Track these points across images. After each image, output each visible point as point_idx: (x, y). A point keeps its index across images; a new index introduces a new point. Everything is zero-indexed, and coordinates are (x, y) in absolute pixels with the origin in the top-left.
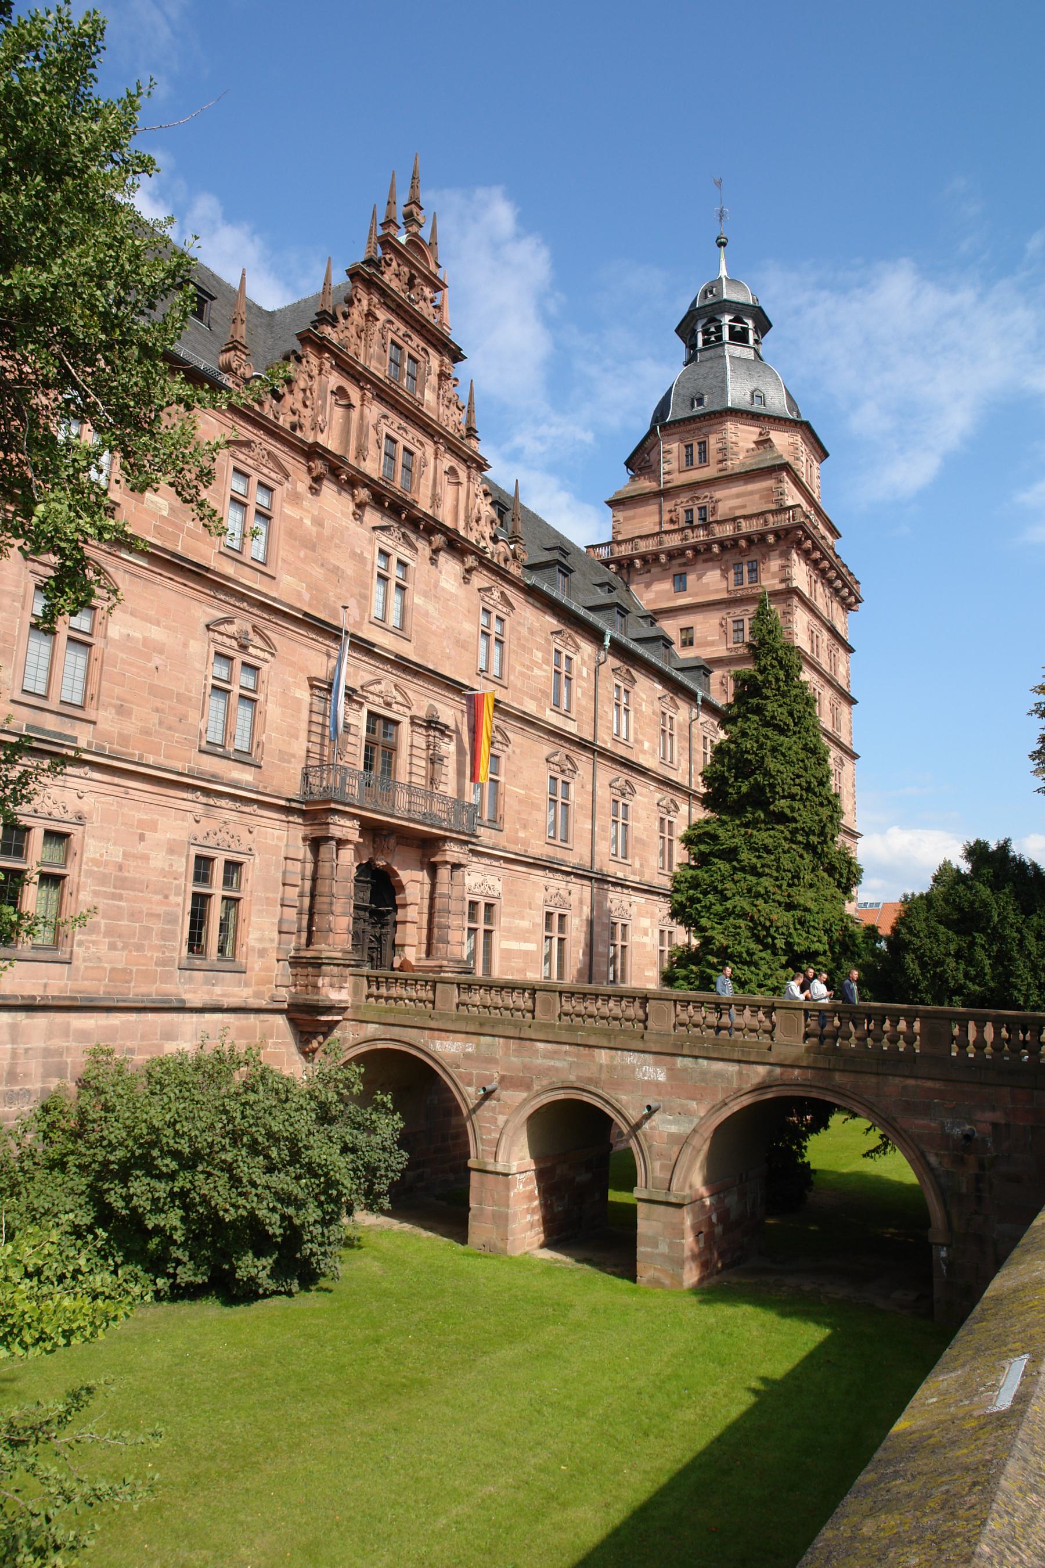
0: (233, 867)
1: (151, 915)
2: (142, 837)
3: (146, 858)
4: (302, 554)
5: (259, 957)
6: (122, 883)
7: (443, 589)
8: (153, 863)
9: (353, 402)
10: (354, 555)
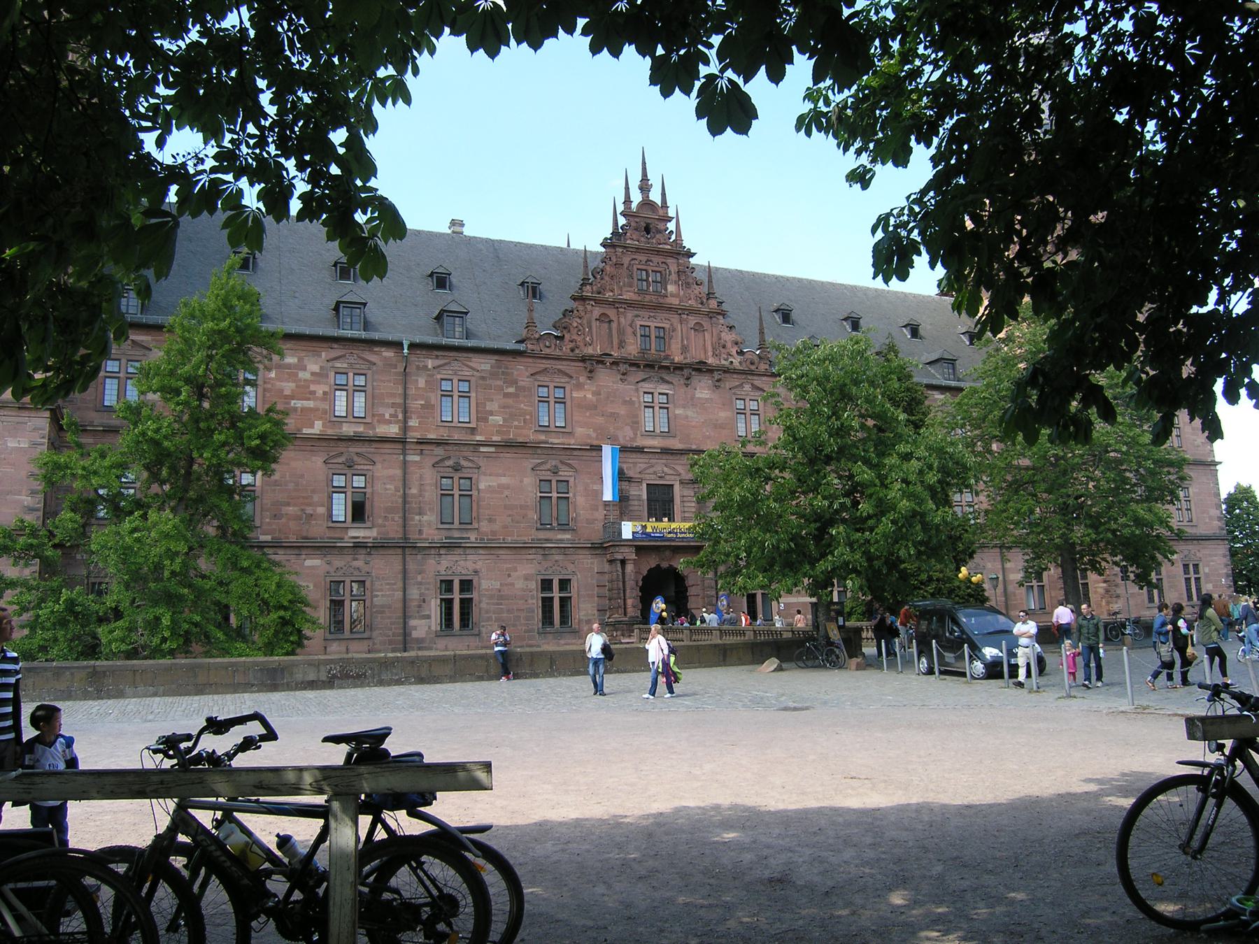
0: (564, 584)
1: (518, 610)
2: (509, 576)
3: (513, 584)
4: (588, 414)
6: (501, 597)
7: (699, 398)
8: (517, 586)
9: (612, 318)
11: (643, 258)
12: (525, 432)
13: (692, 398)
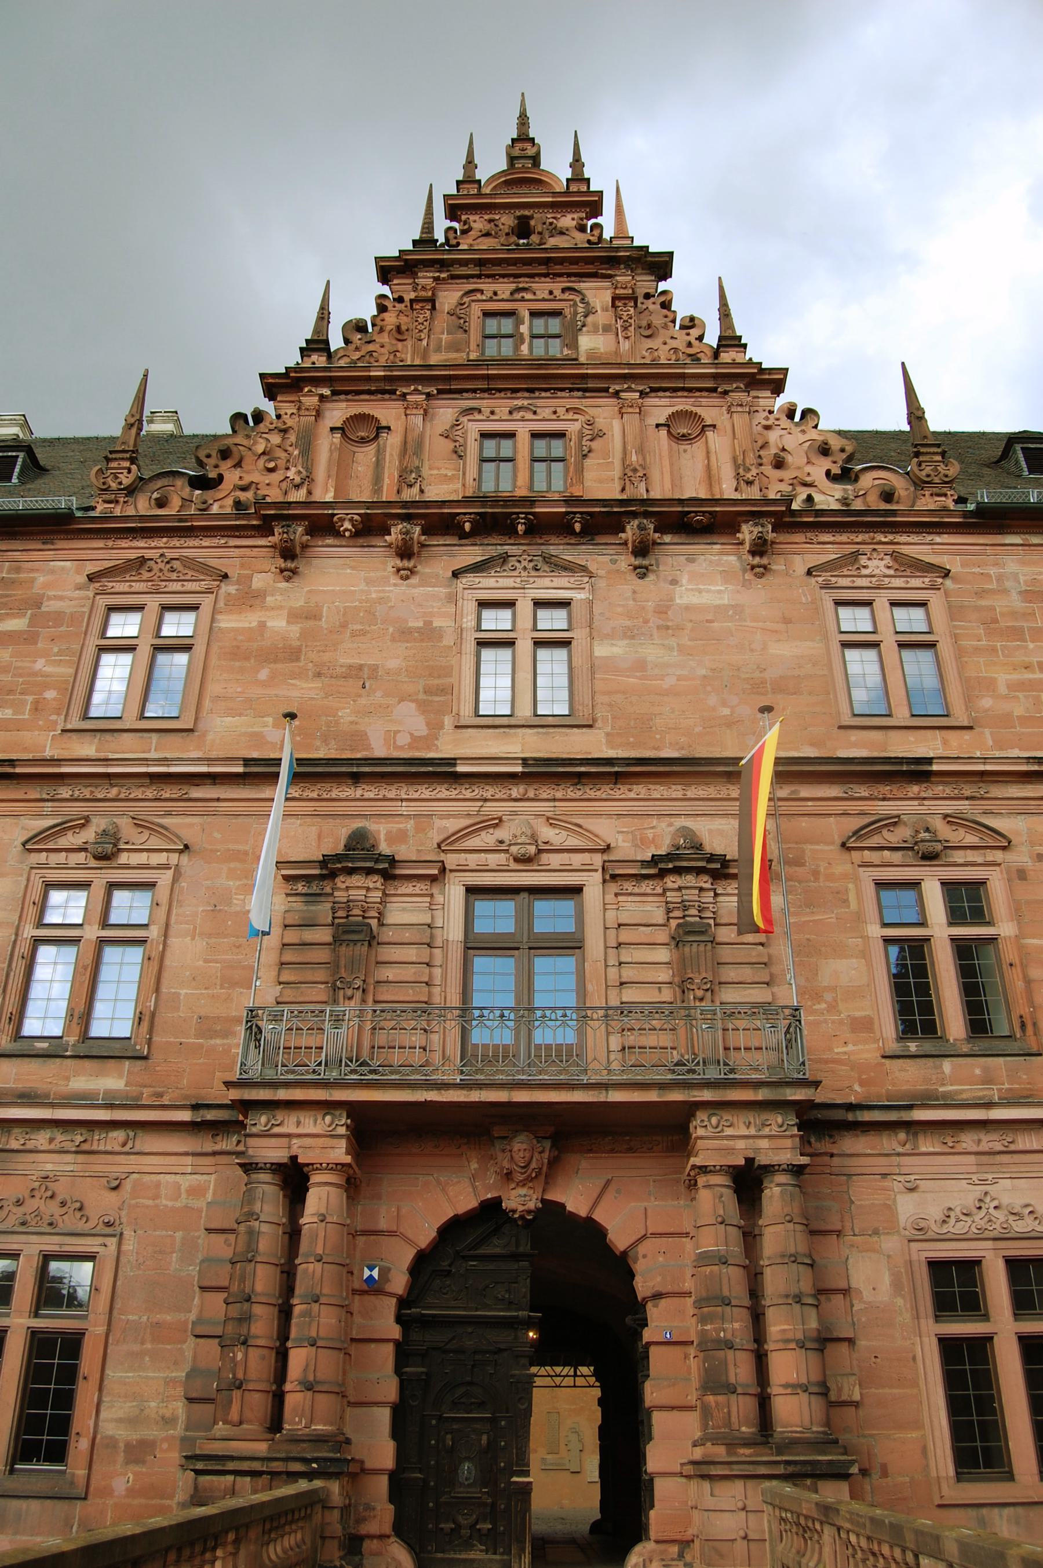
5: (127, 1462)
7: (688, 608)
10: (405, 634)
11: (504, 288)
12: (29, 737)
13: (662, 610)
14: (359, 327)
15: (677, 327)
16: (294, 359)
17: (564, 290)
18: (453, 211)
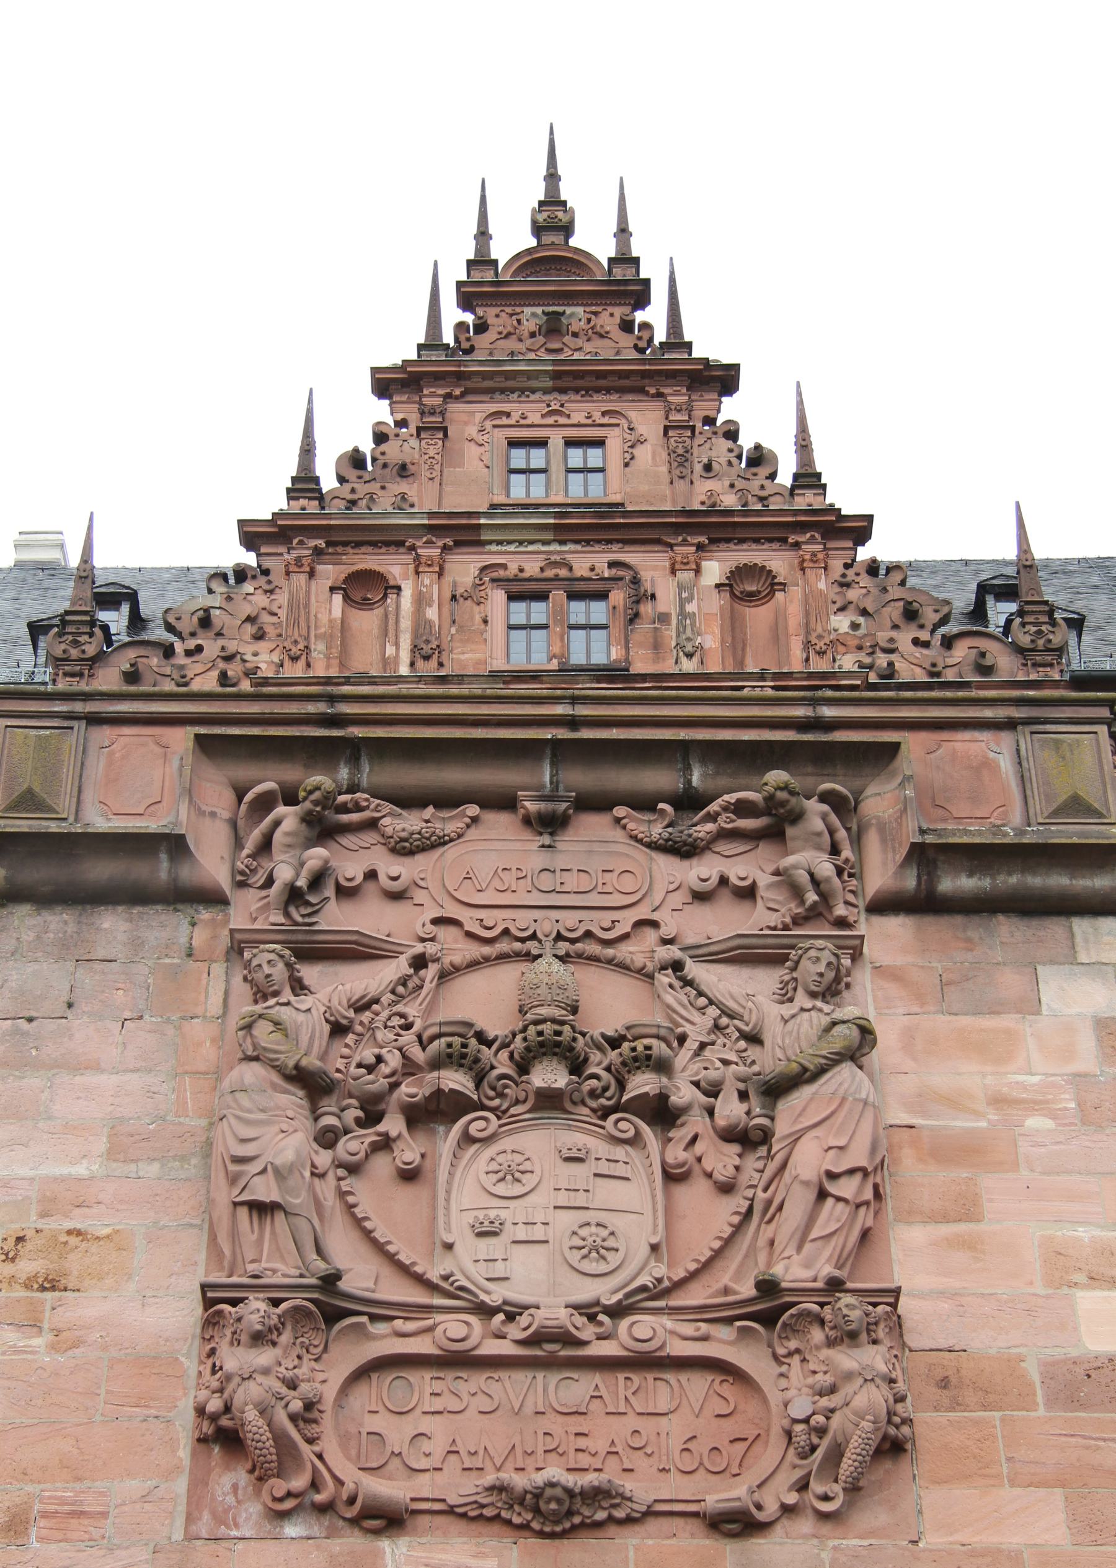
14: (356, 460)
15: (743, 465)
16: (280, 503)
17: (604, 414)
18: (467, 298)
